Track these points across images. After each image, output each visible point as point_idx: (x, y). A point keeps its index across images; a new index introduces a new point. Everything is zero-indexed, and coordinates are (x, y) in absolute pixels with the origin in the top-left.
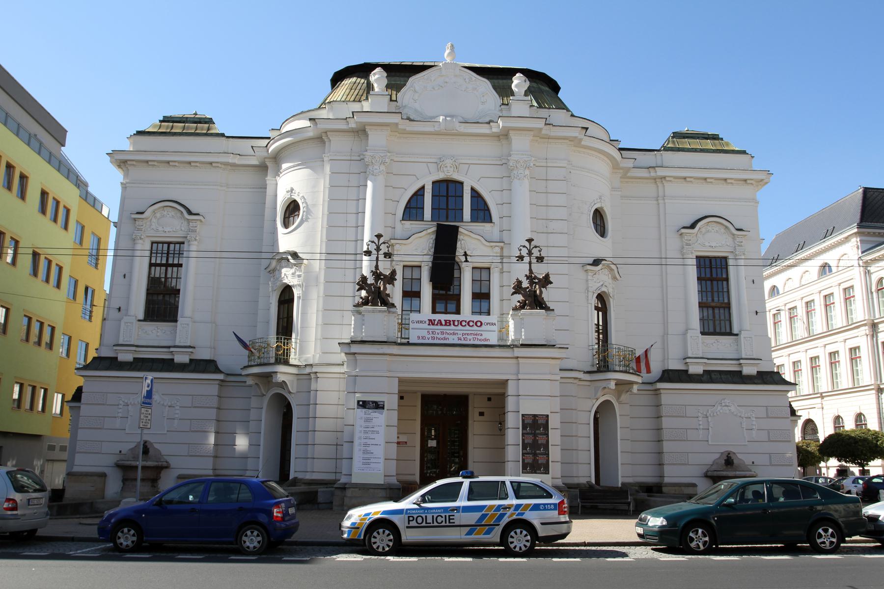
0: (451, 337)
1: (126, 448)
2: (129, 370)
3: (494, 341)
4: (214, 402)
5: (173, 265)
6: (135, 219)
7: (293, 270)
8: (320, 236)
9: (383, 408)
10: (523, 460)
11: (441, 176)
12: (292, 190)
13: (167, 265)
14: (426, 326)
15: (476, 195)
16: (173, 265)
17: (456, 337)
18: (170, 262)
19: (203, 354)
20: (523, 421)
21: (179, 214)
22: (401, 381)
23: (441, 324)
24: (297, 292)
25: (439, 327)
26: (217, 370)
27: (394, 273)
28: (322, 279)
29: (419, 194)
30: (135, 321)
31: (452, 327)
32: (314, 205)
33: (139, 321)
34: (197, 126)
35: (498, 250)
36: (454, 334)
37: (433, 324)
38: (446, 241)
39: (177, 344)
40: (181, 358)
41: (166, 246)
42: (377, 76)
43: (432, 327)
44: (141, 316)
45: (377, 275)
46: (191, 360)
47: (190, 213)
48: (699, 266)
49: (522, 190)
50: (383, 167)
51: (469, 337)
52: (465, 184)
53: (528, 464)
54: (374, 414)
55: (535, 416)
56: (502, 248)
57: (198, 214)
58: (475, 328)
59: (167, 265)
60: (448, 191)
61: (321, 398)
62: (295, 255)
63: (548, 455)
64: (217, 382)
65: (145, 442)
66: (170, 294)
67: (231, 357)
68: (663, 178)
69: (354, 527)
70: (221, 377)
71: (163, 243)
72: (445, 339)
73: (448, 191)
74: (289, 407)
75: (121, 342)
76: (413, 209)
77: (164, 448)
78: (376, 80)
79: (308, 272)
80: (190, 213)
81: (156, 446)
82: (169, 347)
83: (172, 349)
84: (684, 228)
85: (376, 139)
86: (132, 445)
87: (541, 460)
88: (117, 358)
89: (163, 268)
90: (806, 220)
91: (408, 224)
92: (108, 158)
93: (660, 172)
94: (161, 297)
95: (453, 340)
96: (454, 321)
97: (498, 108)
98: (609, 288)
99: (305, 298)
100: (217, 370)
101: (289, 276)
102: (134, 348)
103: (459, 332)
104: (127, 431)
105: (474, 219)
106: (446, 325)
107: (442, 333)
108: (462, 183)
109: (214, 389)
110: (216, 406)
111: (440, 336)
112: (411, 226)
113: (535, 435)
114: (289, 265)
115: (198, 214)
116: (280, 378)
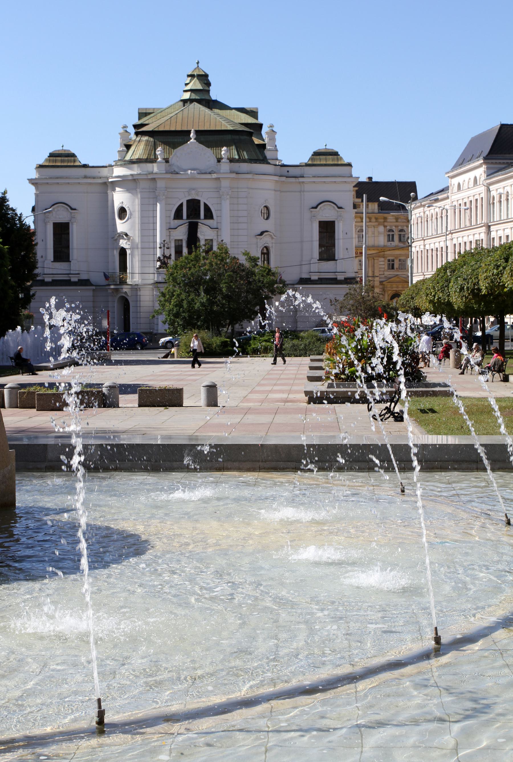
7: (125, 241)
8: (137, 227)
11: (190, 198)
15: (206, 205)
19: (84, 277)
24: (128, 252)
26: (91, 285)
27: (170, 255)
28: (140, 246)
29: (181, 205)
32: (134, 211)
35: (216, 232)
38: (193, 230)
40: (74, 279)
42: (159, 152)
44: (52, 260)
45: (164, 256)
47: (72, 209)
48: (320, 226)
49: (226, 205)
50: (164, 197)
57: (75, 209)
60: (194, 206)
61: (142, 298)
62: (126, 235)
67: (97, 278)
68: (303, 182)
69: (163, 343)
73: (194, 206)
76: (178, 215)
78: (160, 154)
79: (133, 242)
80: (72, 209)
84: (313, 208)
85: (160, 184)
90: (468, 145)
91: (176, 221)
93: (301, 180)
99: (132, 254)
100: (91, 285)
101: (123, 243)
109: (91, 293)
112: (178, 222)
114: (123, 238)
115: (75, 209)
116: (125, 290)
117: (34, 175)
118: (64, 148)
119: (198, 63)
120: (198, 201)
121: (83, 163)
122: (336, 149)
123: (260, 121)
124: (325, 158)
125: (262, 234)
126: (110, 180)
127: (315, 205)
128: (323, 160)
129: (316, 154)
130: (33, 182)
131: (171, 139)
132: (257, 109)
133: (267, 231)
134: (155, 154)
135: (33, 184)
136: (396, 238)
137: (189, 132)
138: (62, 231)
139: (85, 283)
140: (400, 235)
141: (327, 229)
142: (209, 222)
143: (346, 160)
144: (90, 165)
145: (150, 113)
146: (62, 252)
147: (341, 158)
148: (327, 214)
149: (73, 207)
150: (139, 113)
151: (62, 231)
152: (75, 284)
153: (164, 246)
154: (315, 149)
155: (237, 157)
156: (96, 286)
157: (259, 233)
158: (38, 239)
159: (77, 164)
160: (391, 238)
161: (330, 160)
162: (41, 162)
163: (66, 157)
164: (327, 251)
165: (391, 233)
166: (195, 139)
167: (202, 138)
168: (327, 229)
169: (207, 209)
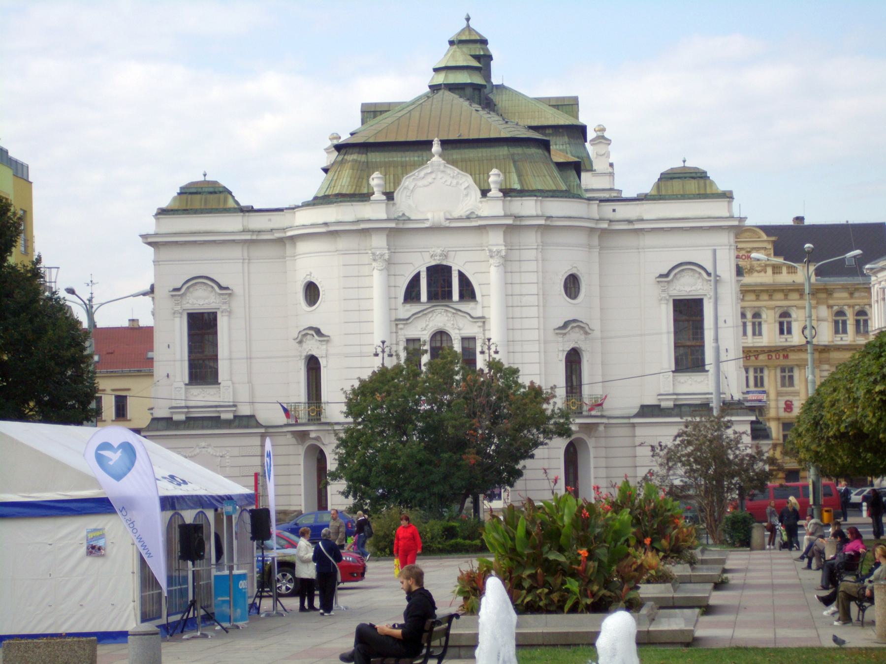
2: (184, 429)
6: (173, 296)
11: (433, 263)
12: (311, 273)
15: (461, 275)
19: (245, 410)
21: (210, 289)
26: (259, 425)
29: (416, 278)
30: (183, 386)
33: (186, 385)
35: (481, 324)
40: (227, 416)
44: (187, 381)
46: (235, 417)
52: (453, 268)
56: (484, 322)
57: (227, 288)
62: (318, 332)
70: (263, 430)
74: (322, 452)
82: (216, 406)
83: (218, 409)
88: (172, 418)
91: (408, 306)
92: (140, 239)
94: (201, 362)
98: (582, 345)
102: (186, 410)
105: (462, 297)
108: (450, 267)
110: (259, 453)
117: (150, 226)
118: (208, 179)
119: (468, 19)
120: (448, 270)
121: (243, 203)
122: (702, 166)
123: (583, 119)
124: (684, 182)
125: (566, 325)
126: (289, 234)
127: (665, 272)
128: (676, 186)
129: (667, 177)
130: (150, 240)
131: (397, 157)
132: (576, 99)
133: (574, 321)
134: (369, 184)
135: (150, 244)
136: (850, 328)
137: (428, 144)
138: (202, 328)
139: (247, 422)
140: (858, 322)
141: (688, 313)
142: (467, 307)
143: (722, 187)
144: (255, 207)
145: (382, 112)
146: (203, 367)
147: (712, 183)
148: (688, 286)
149: (223, 284)
150: (363, 112)
151: (202, 328)
152: (228, 424)
153: (383, 352)
154: (665, 167)
155: (517, 186)
156: (267, 427)
157: (561, 324)
158: (159, 341)
159: (231, 204)
160: (839, 327)
161: (692, 186)
162: (165, 203)
163: (211, 193)
164: (689, 356)
165: (840, 318)
166: (440, 156)
167: (456, 154)
168: (688, 313)
169: (465, 282)
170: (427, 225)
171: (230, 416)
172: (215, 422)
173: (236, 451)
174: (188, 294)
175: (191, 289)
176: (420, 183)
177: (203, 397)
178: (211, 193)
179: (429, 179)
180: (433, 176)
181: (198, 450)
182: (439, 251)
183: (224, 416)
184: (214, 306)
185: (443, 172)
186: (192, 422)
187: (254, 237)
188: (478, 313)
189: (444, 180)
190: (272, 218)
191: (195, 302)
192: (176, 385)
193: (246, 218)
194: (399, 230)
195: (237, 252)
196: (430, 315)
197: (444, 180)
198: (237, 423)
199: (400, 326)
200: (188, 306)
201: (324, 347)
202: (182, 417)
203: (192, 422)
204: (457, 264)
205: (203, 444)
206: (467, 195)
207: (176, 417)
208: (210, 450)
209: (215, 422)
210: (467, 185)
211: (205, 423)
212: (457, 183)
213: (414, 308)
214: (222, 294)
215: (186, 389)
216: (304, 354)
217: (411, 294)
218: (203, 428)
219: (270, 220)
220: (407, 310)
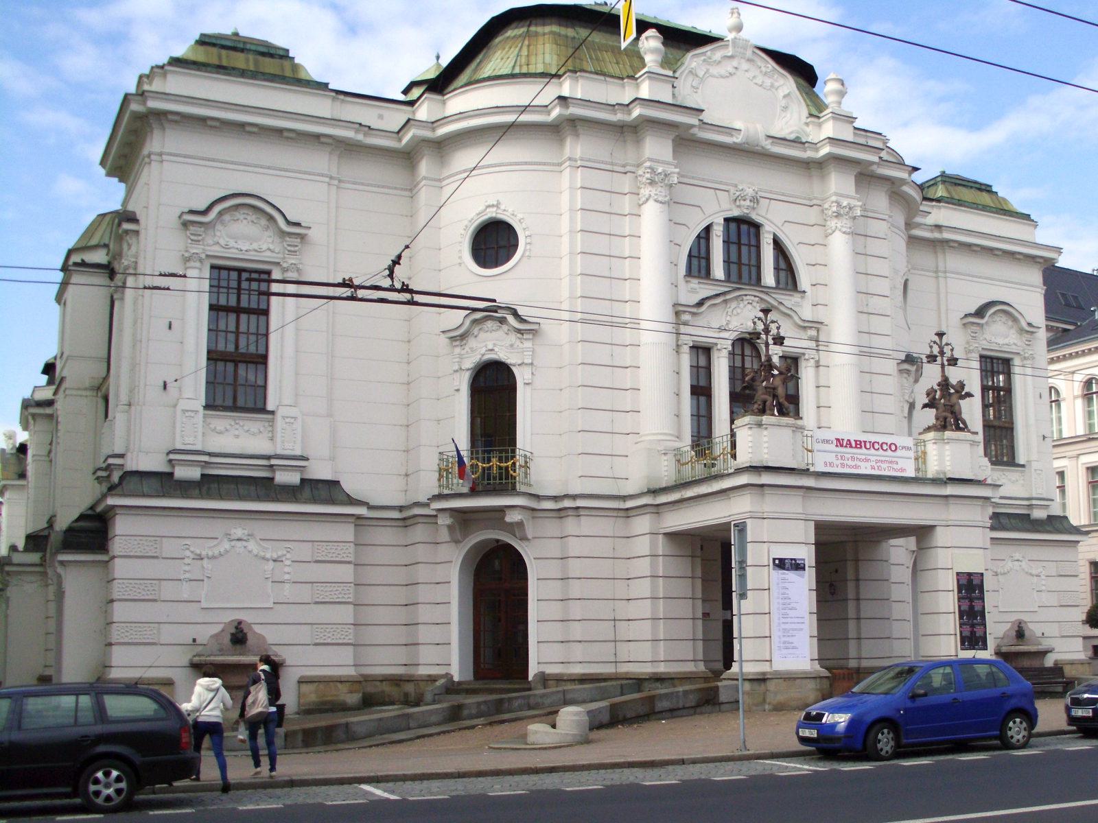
0: (862, 464)
1: (205, 634)
3: (911, 473)
4: (348, 552)
5: (249, 311)
9: (804, 569)
10: (961, 632)
11: (736, 213)
13: (238, 310)
14: (832, 447)
16: (249, 311)
17: (868, 465)
18: (244, 304)
19: (320, 471)
20: (958, 581)
21: (264, 222)
22: (821, 527)
23: (851, 447)
25: (849, 450)
26: (352, 501)
31: (864, 450)
34: (264, 61)
36: (867, 460)
37: (842, 446)
39: (279, 451)
41: (234, 275)
43: (840, 449)
51: (884, 466)
53: (965, 637)
54: (791, 575)
55: (970, 574)
56: (818, 331)
57: (298, 224)
58: (889, 453)
59: (238, 310)
63: (984, 625)
64: (352, 520)
65: (240, 623)
66: (247, 362)
70: (362, 511)
71: (229, 269)
72: (857, 467)
75: (179, 446)
77: (272, 634)
81: (257, 629)
82: (269, 458)
83: (273, 462)
86: (217, 629)
87: (979, 633)
88: (171, 474)
89: (232, 317)
91: (694, 283)
95: (865, 469)
96: (865, 442)
97: (804, 119)
100: (352, 501)
102: (206, 458)
103: (873, 458)
104: (204, 605)
106: (856, 447)
107: (853, 459)
111: (850, 463)
113: (971, 600)
120: (757, 227)
126: (443, 131)
139: (328, 491)
163: (263, 54)
170: (737, 139)
171: (293, 478)
172: (264, 487)
173: (305, 552)
174: (219, 227)
175: (227, 217)
176: (714, 70)
177: (237, 438)
178: (263, 54)
179: (728, 67)
180: (735, 63)
181: (226, 545)
182: (750, 192)
183: (282, 478)
184: (267, 256)
185: (749, 60)
186: (211, 485)
187: (360, 137)
188: (807, 313)
189: (750, 74)
190: (386, 113)
191: (232, 243)
192: (183, 405)
193: (338, 103)
194: (690, 138)
195: (320, 161)
196: (734, 305)
197: (750, 74)
198: (307, 492)
199: (686, 317)
200: (216, 250)
201: (528, 344)
202: (194, 473)
203: (214, 486)
204: (775, 220)
205: (239, 532)
206: (785, 108)
207: (181, 473)
208: (252, 545)
209: (264, 487)
210: (787, 92)
211: (243, 490)
212: (772, 86)
213: (705, 290)
214: (290, 234)
215: (205, 416)
216: (471, 362)
217: (698, 263)
218: (241, 498)
219: (381, 117)
220: (693, 291)
